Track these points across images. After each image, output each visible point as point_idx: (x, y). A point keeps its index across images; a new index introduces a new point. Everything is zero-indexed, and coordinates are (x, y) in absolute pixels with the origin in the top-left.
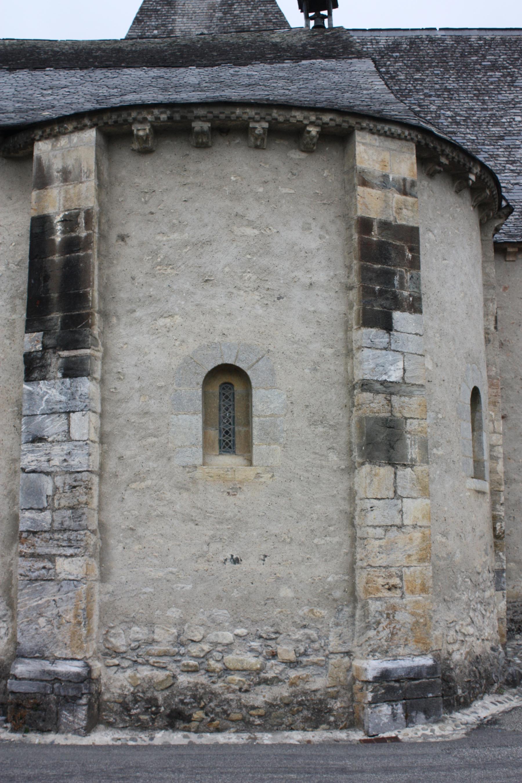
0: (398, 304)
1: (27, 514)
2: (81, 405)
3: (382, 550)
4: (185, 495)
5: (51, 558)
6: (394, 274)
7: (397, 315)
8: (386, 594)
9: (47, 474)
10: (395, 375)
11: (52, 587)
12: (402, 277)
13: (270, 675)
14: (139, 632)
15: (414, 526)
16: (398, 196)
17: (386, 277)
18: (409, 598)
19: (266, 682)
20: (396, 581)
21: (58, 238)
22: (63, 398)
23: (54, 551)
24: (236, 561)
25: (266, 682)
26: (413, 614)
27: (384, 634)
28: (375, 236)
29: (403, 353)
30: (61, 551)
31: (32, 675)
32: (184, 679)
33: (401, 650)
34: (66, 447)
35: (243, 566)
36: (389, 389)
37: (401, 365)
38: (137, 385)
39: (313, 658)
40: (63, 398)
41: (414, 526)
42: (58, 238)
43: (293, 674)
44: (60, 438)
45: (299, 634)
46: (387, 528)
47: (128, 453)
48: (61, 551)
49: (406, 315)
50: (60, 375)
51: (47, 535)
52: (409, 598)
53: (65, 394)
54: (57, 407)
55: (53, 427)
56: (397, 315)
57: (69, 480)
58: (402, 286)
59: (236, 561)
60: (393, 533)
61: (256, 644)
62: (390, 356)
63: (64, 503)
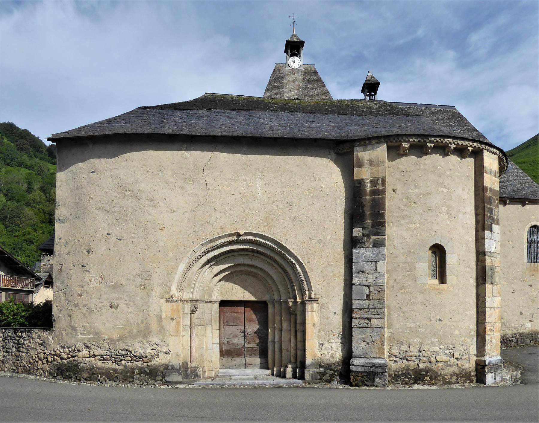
1: (356, 302)
2: (382, 259)
4: (422, 295)
5: (369, 319)
9: (366, 286)
11: (370, 330)
13: (451, 363)
14: (404, 348)
19: (450, 366)
21: (368, 189)
22: (373, 256)
23: (370, 317)
24: (441, 320)
25: (450, 366)
30: (373, 316)
31: (363, 364)
32: (421, 365)
34: (375, 275)
35: (443, 322)
38: (402, 251)
39: (465, 357)
40: (373, 256)
42: (368, 189)
44: (372, 271)
45: (461, 348)
47: (398, 278)
48: (373, 316)
50: (371, 246)
51: (367, 310)
53: (374, 254)
54: (370, 259)
55: (368, 267)
57: (377, 288)
59: (441, 320)
61: (447, 352)
63: (374, 297)
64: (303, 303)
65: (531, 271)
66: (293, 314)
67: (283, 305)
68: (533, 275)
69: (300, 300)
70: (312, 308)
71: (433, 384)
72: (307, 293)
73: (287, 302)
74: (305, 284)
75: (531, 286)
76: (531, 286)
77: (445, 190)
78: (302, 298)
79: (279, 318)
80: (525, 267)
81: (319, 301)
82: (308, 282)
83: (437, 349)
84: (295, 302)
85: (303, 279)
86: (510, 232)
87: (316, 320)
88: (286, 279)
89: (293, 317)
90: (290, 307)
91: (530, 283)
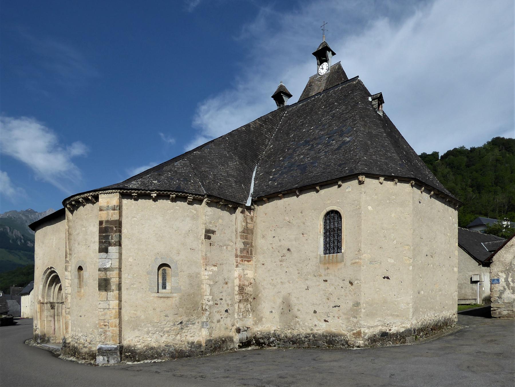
0: (110, 244)
3: (102, 315)
6: (109, 235)
7: (110, 248)
8: (104, 327)
10: (108, 266)
12: (112, 236)
13: (85, 345)
15: (113, 309)
16: (112, 211)
17: (107, 237)
18: (111, 328)
20: (107, 324)
26: (112, 333)
27: (103, 338)
28: (104, 225)
29: (111, 259)
32: (76, 345)
33: (108, 342)
36: (106, 270)
37: (110, 262)
41: (113, 309)
43: (89, 346)
45: (90, 336)
46: (104, 309)
49: (113, 247)
52: (111, 328)
56: (110, 248)
58: (112, 239)
60: (106, 311)
62: (107, 260)
65: (325, 264)
68: (328, 268)
71: (78, 358)
75: (326, 281)
76: (326, 281)
77: (84, 229)
80: (318, 261)
83: (80, 335)
86: (304, 223)
91: (325, 279)
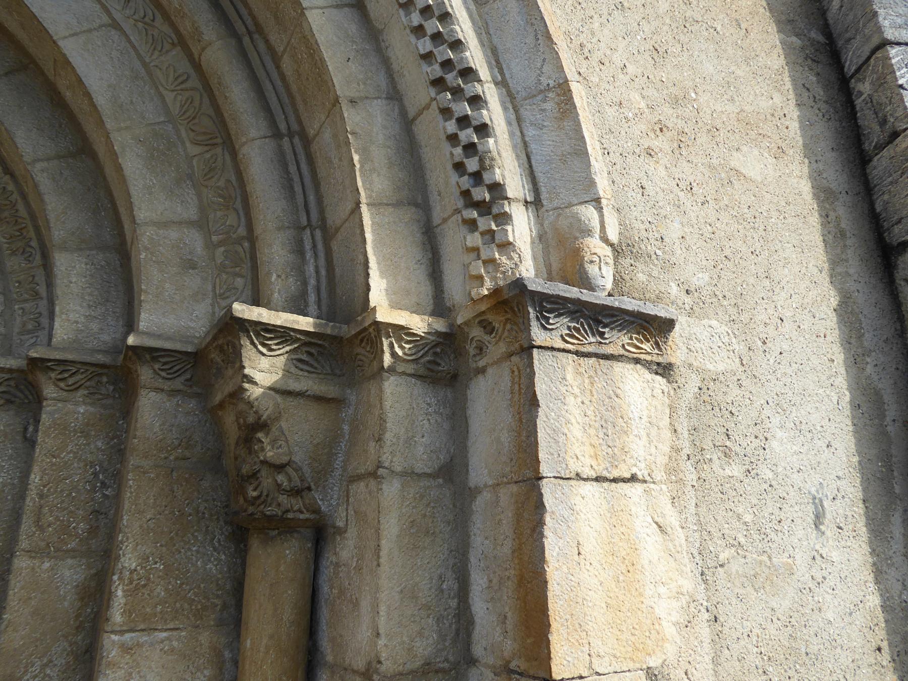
64: (486, 341)
66: (282, 526)
67: (155, 410)
69: (419, 324)
70: (610, 421)
72: (521, 228)
73: (209, 361)
74: (495, 113)
78: (439, 307)
79: (71, 574)
81: (677, 351)
82: (547, 99)
84: (342, 349)
85: (475, 56)
87: (668, 612)
88: (237, 95)
89: (274, 568)
90: (255, 427)
